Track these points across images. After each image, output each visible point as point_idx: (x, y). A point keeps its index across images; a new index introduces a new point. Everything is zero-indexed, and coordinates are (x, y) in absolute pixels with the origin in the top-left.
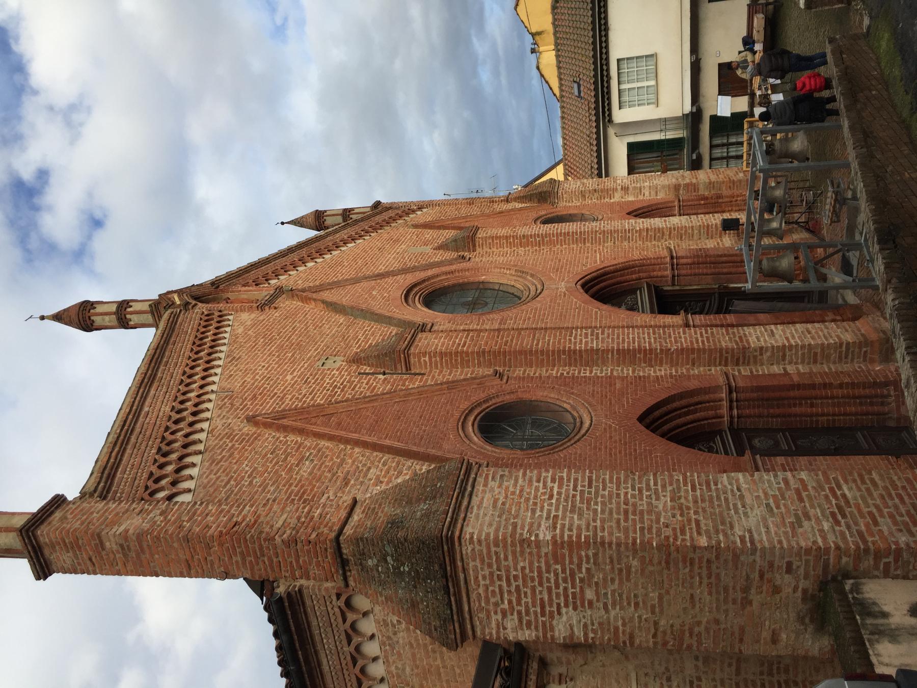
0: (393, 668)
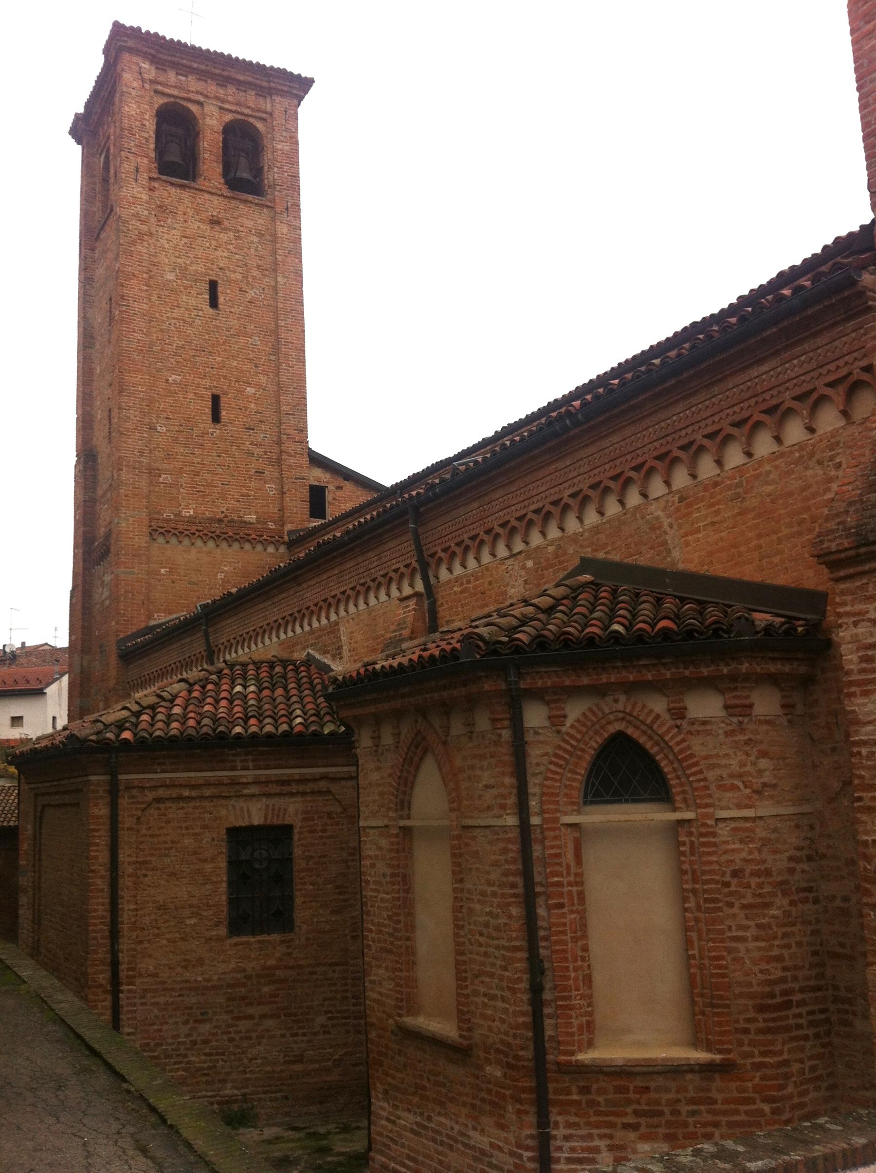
0: (767, 467)
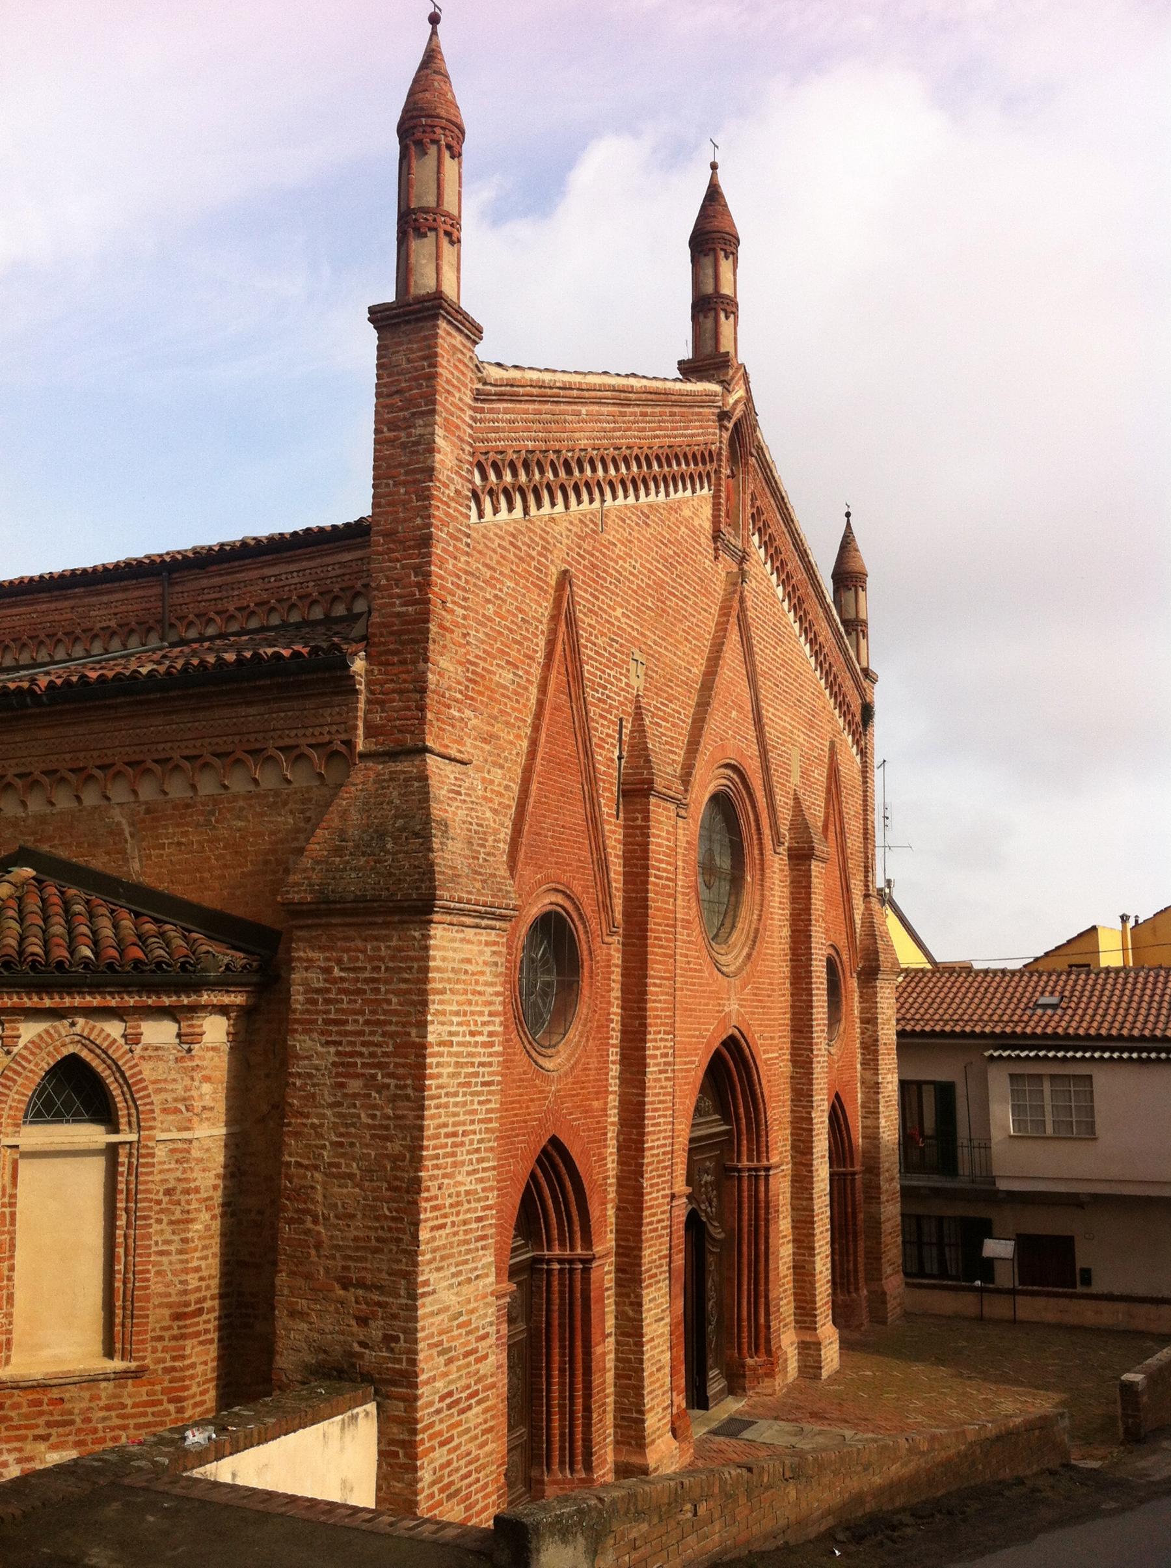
0: (241, 803)
